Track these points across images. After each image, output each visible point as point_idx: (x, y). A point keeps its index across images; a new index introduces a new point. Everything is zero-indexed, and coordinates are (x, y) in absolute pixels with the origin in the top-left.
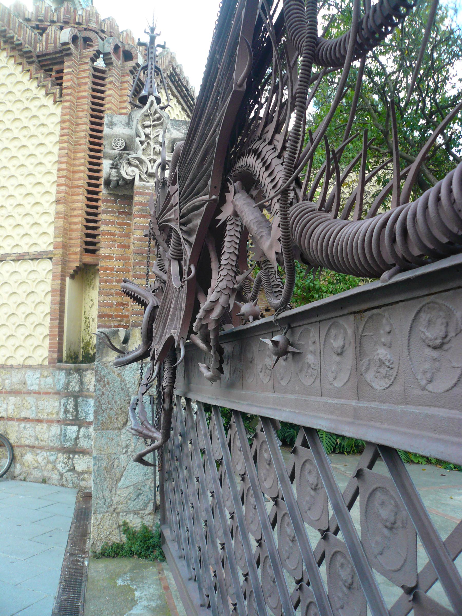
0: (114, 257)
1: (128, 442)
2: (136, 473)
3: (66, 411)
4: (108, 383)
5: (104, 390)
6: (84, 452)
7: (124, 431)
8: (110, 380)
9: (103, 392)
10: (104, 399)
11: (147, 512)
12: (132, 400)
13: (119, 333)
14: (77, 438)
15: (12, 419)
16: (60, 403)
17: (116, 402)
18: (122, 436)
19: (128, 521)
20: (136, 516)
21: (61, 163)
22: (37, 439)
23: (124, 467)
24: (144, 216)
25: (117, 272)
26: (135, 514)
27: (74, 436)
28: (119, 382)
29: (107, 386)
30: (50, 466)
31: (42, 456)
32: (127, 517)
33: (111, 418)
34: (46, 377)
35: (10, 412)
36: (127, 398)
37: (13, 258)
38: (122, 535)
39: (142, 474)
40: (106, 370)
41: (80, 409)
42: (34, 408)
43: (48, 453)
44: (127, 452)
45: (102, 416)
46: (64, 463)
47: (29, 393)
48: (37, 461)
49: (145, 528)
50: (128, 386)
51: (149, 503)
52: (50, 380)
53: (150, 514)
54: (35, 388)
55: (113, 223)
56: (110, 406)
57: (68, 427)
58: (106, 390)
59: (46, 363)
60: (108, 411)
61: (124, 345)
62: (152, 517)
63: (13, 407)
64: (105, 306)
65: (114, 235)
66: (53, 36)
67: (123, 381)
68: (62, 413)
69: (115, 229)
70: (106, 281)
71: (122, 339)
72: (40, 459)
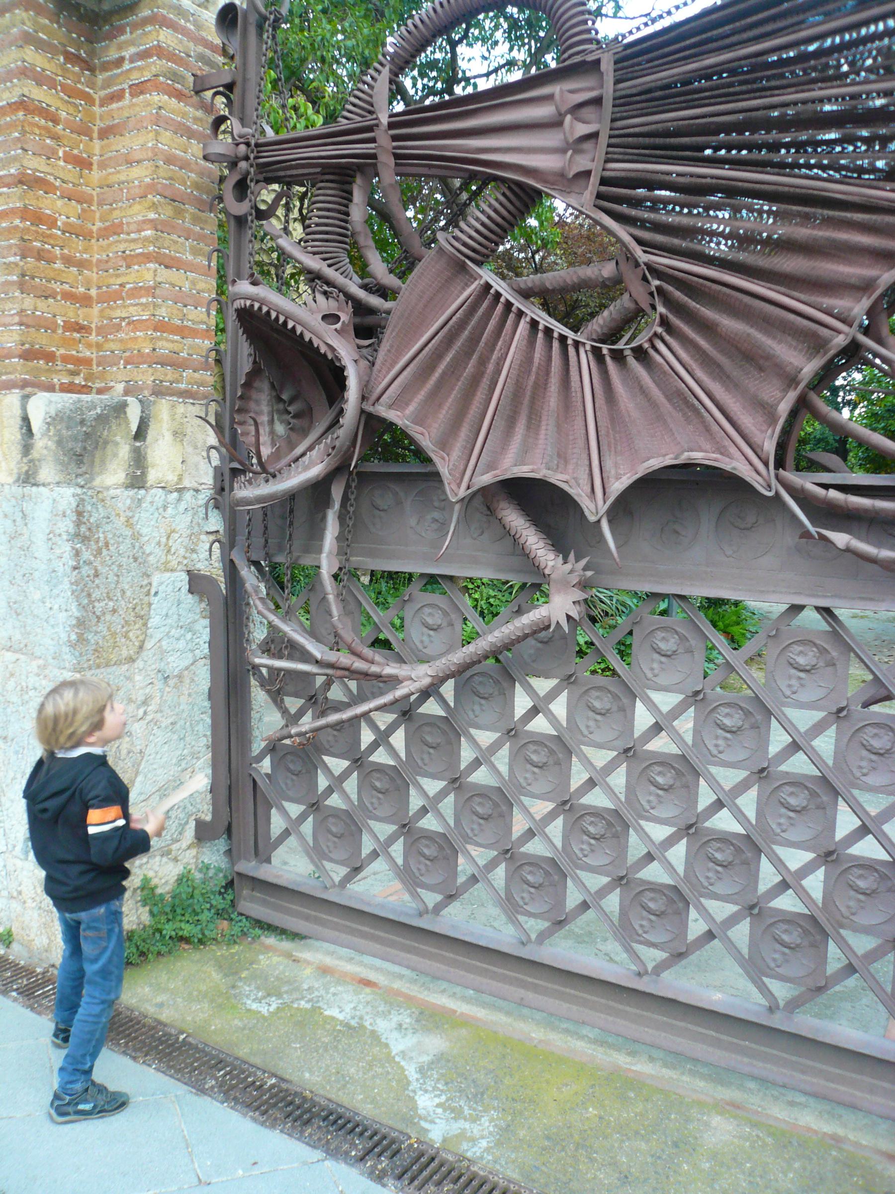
0: (56, 188)
1: (147, 691)
2: (164, 760)
4: (107, 545)
5: (97, 564)
7: (139, 664)
8: (110, 536)
9: (96, 571)
10: (98, 587)
11: (184, 846)
12: (155, 584)
13: (129, 410)
17: (123, 592)
18: (137, 678)
19: (151, 874)
20: (165, 859)
23: (141, 752)
24: (179, 96)
25: (64, 232)
26: (162, 856)
28: (128, 541)
29: (105, 552)
32: (149, 866)
33: (114, 635)
36: (145, 582)
38: (141, 910)
39: (174, 761)
40: (101, 510)
44: (145, 713)
45: (96, 633)
49: (182, 880)
50: (148, 549)
51: (187, 823)
53: (189, 848)
55: (52, 85)
56: (111, 604)
58: (103, 563)
60: (108, 617)
61: (138, 444)
62: (193, 852)
64: (38, 327)
65: (56, 121)
67: (136, 536)
69: (59, 104)
70: (40, 255)
71: (134, 427)
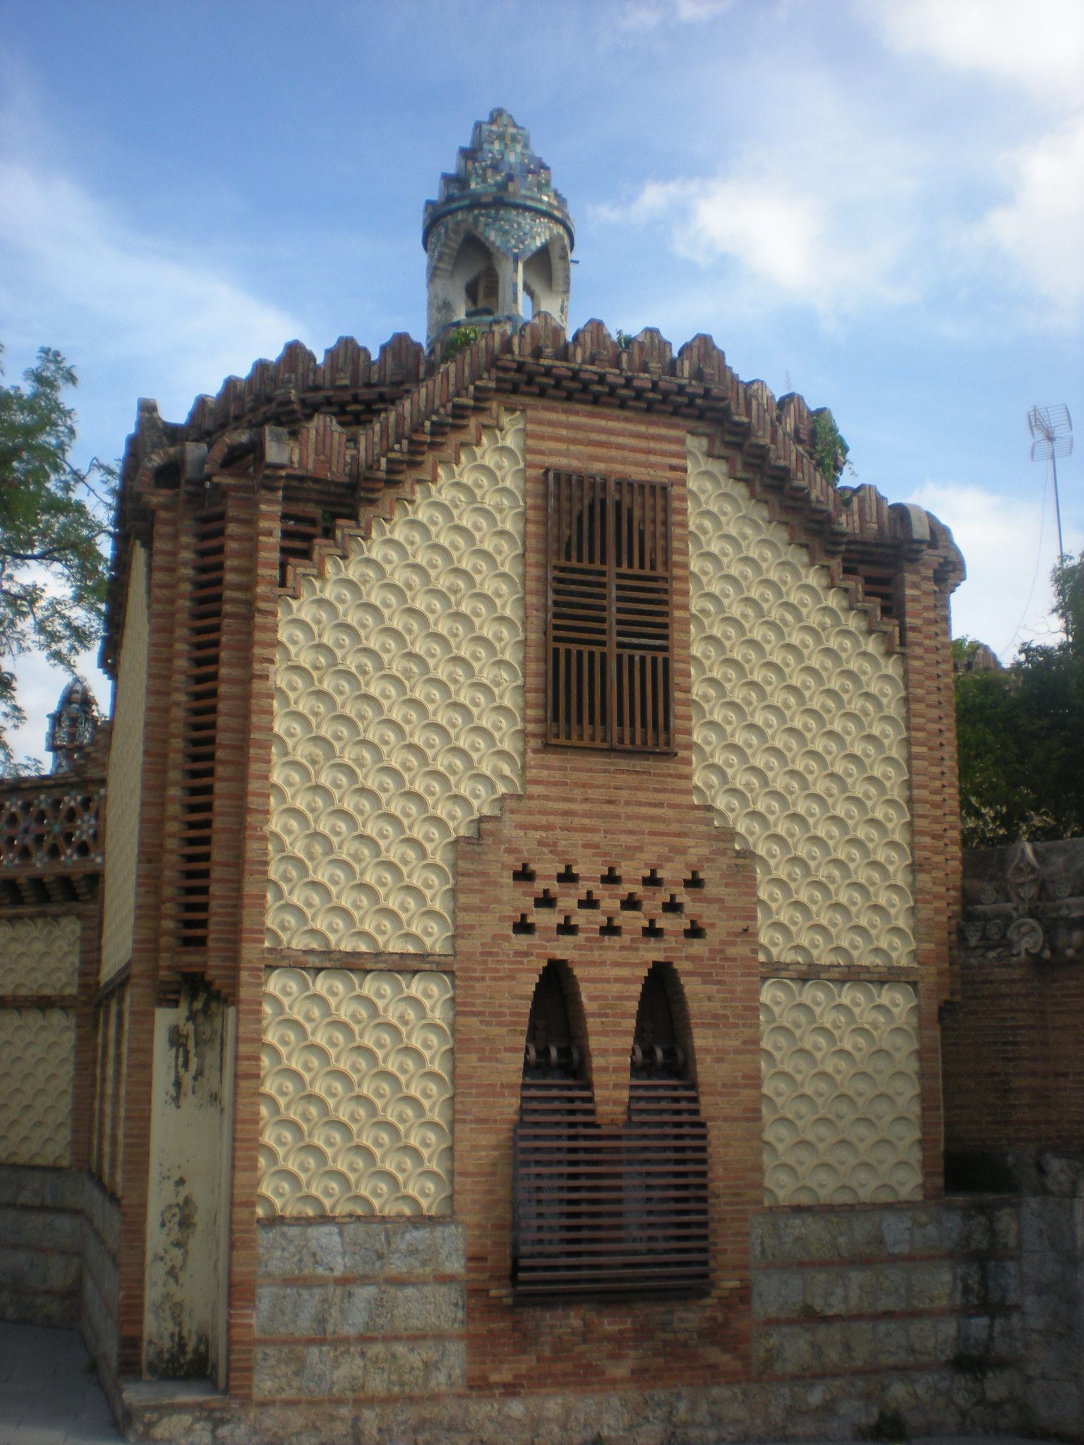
3: (967, 1290)
6: (1001, 1364)
14: (991, 1338)
15: (858, 1317)
16: (955, 1275)
21: (919, 787)
22: (912, 1351)
27: (984, 1335)
30: (941, 1401)
31: (923, 1385)
34: (923, 1226)
35: (853, 1302)
37: (836, 976)
41: (991, 1284)
42: (902, 1290)
43: (936, 1377)
46: (967, 1391)
47: (893, 1259)
48: (915, 1395)
52: (931, 1230)
54: (904, 1249)
57: (973, 1321)
59: (919, 1197)
63: (858, 1291)
66: (874, 509)
68: (958, 1296)
72: (920, 1390)
